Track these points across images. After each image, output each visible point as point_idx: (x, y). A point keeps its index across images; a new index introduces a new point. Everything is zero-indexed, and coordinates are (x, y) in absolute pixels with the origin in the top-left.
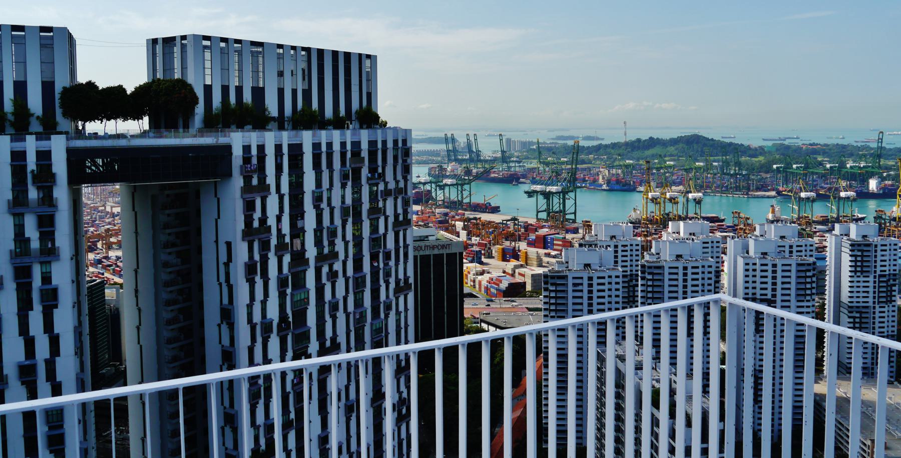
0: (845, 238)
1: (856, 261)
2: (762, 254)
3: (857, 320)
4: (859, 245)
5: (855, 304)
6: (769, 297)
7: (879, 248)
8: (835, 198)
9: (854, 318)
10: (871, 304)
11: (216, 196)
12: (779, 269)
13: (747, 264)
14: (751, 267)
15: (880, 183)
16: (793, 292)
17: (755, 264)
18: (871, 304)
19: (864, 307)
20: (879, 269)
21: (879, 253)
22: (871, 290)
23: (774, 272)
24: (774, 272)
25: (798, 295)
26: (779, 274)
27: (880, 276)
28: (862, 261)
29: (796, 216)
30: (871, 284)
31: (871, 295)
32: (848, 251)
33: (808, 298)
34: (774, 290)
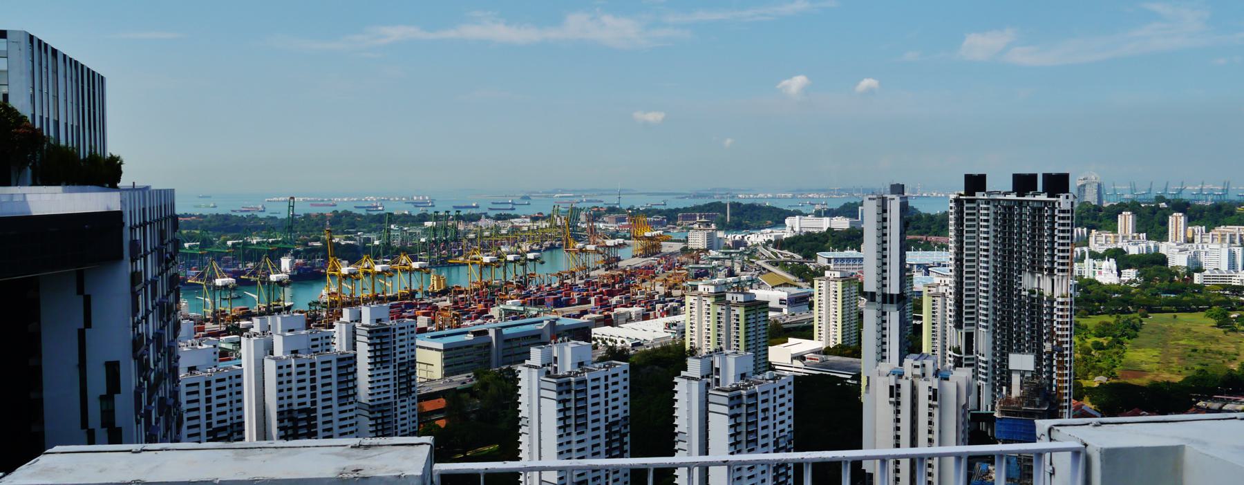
0: (357, 325)
1: (374, 351)
2: (293, 352)
3: (380, 421)
4: (378, 331)
5: (376, 403)
6: (308, 405)
7: (398, 332)
8: (263, 283)
9: (376, 419)
10: (392, 400)
11: (80, 290)
12: (318, 368)
13: (280, 367)
14: (285, 371)
15: (293, 261)
16: (334, 395)
17: (289, 366)
18: (392, 400)
19: (386, 404)
20: (398, 356)
21: (398, 338)
22: (391, 382)
23: (313, 373)
24: (313, 373)
25: (340, 398)
26: (319, 375)
27: (400, 365)
28: (381, 350)
29: (210, 311)
30: (391, 376)
31: (392, 388)
32: (365, 339)
33: (351, 399)
34: (313, 396)
